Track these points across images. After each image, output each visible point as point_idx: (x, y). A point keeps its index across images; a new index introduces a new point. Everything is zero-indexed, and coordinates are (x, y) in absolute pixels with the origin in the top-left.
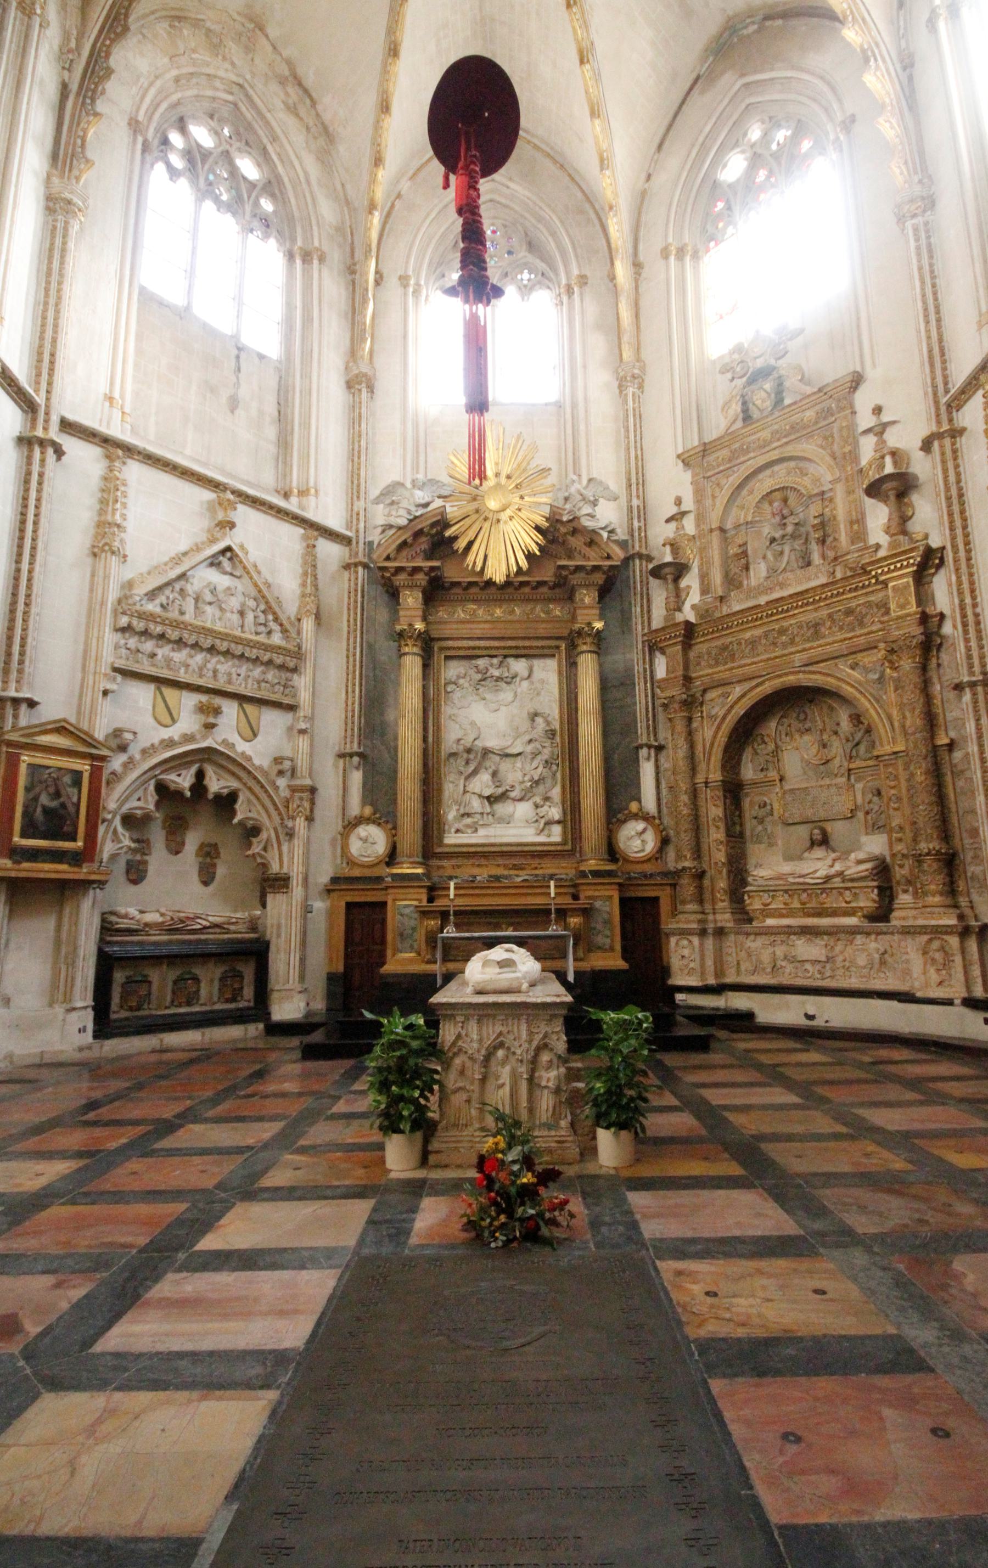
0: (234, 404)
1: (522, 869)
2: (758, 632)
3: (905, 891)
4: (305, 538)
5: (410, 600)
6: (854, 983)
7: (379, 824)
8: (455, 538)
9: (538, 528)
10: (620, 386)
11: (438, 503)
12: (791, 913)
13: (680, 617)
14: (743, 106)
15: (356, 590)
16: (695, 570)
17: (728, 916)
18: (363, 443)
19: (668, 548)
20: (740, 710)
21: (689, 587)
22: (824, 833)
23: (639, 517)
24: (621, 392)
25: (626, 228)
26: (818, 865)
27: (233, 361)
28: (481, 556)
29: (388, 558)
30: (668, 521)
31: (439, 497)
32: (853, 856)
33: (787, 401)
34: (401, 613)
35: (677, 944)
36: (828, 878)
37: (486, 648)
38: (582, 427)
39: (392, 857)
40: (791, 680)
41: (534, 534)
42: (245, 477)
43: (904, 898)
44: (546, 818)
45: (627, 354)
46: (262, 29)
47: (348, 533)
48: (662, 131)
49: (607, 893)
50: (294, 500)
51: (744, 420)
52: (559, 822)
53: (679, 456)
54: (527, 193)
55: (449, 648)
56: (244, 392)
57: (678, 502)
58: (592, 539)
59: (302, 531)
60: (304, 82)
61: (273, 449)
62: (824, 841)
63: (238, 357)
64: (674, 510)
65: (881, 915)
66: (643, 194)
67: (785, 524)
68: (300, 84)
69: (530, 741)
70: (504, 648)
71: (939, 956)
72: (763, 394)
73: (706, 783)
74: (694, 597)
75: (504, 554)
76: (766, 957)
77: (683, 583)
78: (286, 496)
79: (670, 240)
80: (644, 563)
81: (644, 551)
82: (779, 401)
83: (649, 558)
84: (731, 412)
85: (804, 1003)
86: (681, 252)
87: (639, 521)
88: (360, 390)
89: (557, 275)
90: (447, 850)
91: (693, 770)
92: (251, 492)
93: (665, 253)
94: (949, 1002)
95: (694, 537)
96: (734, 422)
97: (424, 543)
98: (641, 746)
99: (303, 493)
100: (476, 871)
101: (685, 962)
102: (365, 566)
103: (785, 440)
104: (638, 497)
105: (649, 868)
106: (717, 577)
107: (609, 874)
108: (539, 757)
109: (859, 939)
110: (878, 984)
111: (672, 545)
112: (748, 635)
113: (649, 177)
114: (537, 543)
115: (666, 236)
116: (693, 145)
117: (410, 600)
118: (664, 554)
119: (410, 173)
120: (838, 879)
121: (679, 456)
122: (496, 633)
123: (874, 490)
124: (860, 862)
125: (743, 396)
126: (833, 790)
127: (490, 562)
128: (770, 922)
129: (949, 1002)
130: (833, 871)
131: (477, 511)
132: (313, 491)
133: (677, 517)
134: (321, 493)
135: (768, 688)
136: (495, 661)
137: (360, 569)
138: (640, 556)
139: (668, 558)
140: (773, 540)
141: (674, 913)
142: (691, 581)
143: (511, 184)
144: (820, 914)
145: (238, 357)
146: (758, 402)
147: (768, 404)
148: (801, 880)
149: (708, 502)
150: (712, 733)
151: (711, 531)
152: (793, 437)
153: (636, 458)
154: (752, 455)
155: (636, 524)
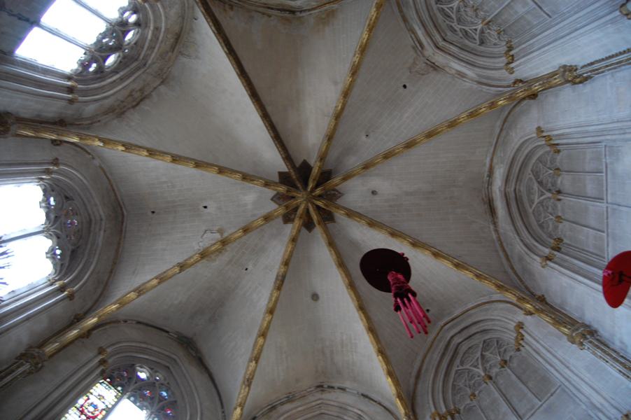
14: (168, 365)
46: (162, 83)
48: (145, 321)
54: (100, 244)
60: (142, 103)
63: (27, 20)
66: (117, 322)
68: (141, 100)
79: (109, 350)
93: (101, 351)
113: (126, 321)
115: (109, 347)
116: (145, 343)
119: (103, 166)
143: (102, 232)
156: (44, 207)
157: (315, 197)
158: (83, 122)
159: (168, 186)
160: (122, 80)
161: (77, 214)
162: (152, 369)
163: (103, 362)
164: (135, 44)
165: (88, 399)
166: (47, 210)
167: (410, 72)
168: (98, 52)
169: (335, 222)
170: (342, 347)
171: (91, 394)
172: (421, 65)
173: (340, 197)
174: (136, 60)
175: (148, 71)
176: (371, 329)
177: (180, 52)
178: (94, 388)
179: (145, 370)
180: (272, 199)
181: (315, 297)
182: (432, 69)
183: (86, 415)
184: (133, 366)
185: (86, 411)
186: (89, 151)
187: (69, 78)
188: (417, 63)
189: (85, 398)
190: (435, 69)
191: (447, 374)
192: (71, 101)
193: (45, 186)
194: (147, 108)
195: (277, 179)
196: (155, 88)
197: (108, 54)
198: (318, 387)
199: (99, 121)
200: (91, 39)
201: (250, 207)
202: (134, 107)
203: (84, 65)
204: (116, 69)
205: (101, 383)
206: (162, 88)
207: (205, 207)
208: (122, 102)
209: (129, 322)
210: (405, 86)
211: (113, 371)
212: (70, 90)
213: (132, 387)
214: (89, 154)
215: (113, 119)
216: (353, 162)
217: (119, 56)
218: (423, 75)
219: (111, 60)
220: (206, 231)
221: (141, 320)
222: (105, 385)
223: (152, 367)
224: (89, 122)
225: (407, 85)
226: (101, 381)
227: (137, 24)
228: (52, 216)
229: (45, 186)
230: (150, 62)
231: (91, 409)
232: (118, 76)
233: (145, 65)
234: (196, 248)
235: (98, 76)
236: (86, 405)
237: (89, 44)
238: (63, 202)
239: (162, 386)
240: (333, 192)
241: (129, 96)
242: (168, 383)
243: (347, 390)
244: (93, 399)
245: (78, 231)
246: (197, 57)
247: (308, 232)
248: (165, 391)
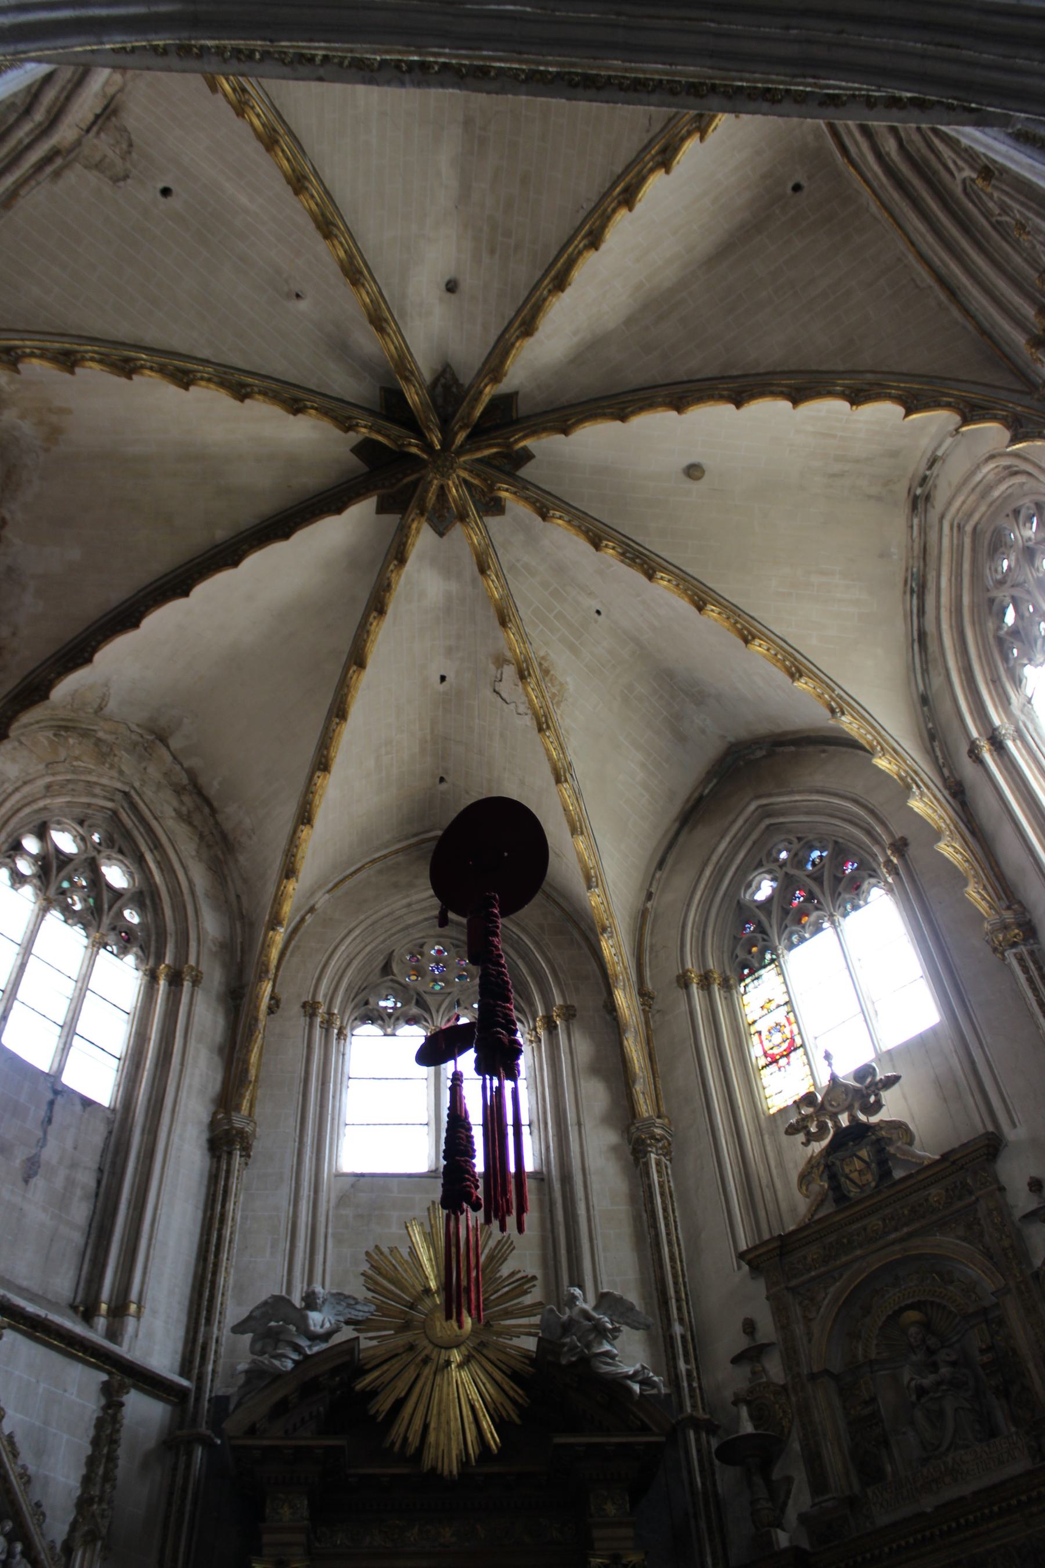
0: (31, 1169)
4: (107, 1389)
5: (286, 1512)
8: (372, 1394)
9: (515, 1376)
10: (635, 1152)
11: (347, 1333)
13: (783, 1539)
15: (184, 1490)
16: (796, 1446)
18: (227, 1233)
19: (744, 1412)
21: (789, 1480)
23: (686, 1355)
24: (637, 1160)
25: (627, 951)
27: (44, 1107)
28: (417, 1424)
29: (252, 1431)
31: (348, 1322)
34: (266, 1538)
38: (582, 1211)
41: (508, 1384)
42: (25, 1284)
45: (645, 1108)
47: (185, 1383)
50: (101, 1322)
51: (837, 1201)
53: (741, 1256)
56: (50, 1154)
57: (749, 1327)
59: (105, 1377)
61: (78, 1238)
63: (51, 1104)
64: (742, 1343)
66: (644, 913)
72: (858, 1164)
74: (800, 1500)
75: (455, 1425)
77: (776, 1475)
78: (88, 1315)
80: (704, 1435)
81: (701, 1414)
82: (885, 1174)
83: (711, 1428)
84: (815, 1187)
86: (706, 982)
87: (687, 1362)
88: (230, 1154)
89: (531, 1004)
92: (31, 1308)
95: (784, 1387)
96: (820, 1204)
99: (119, 1310)
102: (207, 1443)
103: (905, 1230)
104: (681, 1320)
106: (835, 1460)
111: (748, 1403)
113: (649, 896)
116: (705, 865)
117: (286, 1512)
118: (738, 1418)
121: (741, 1256)
125: (827, 1166)
127: (432, 1438)
131: (411, 1347)
132: (133, 1307)
133: (750, 1356)
134: (146, 1312)
137: (199, 1452)
138: (696, 1424)
139: (748, 1428)
140: (921, 1391)
142: (792, 1467)
145: (51, 1104)
146: (855, 1176)
149: (799, 1329)
151: (813, 1377)
152: (916, 1225)
153: (672, 1258)
154: (859, 1252)
155: (682, 1366)
156: (394, 1029)
157: (446, 443)
158: (239, 940)
159: (387, 753)
160: (156, 845)
161: (422, 946)
162: (760, 864)
163: (706, 982)
164: (81, 823)
165: (760, 1033)
166: (401, 1022)
167: (126, 177)
168: (99, 916)
169: (516, 393)
170: (834, 437)
171: (754, 1022)
172: (102, 145)
173: (453, 374)
174: (115, 813)
175: (137, 784)
176: (800, 389)
177: (96, 712)
178: (747, 1010)
179: (758, 879)
180: (441, 534)
181: (694, 471)
182: (113, 119)
183: (782, 1056)
184: (740, 906)
185: (776, 1051)
186: (298, 918)
187: (152, 977)
188: (98, 157)
189: (755, 1039)
190: (115, 112)
191: (965, 225)
192: (196, 982)
193: (356, 1019)
194: (216, 783)
195: (392, 520)
196: (175, 758)
197: (104, 888)
198: (914, 507)
199: (238, 897)
200: (76, 937)
201: (454, 587)
202: (214, 811)
203: (127, 940)
204: (136, 861)
205: (745, 992)
206: (176, 743)
207: (443, 678)
208: (201, 837)
209: (653, 890)
210: (166, 192)
211: (733, 956)
212: (175, 979)
213: (774, 933)
214: (302, 920)
215: (236, 861)
216: (366, 341)
217: (109, 858)
218: (131, 145)
219: (115, 876)
220: (495, 691)
221: (657, 858)
222: (751, 986)
223: (760, 860)
224: (238, 925)
225: (161, 185)
226: (742, 990)
227: (42, 833)
228: (415, 1010)
229: (356, 1019)
230: (119, 785)
231: (777, 1038)
232: (149, 858)
233: (126, 794)
234: (529, 723)
235: (148, 902)
236: (767, 1045)
237: (85, 942)
238: (392, 980)
239: (798, 860)
240: (439, 389)
241: (190, 823)
242: (799, 839)
243: (939, 453)
244: (763, 1026)
245: (456, 946)
246: (106, 685)
247: (533, 461)
248: (812, 852)
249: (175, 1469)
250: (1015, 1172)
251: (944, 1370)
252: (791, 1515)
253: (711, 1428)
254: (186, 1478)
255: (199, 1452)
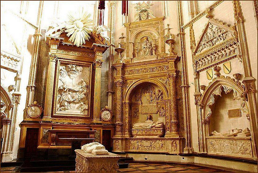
1: (77, 121)
2: (139, 68)
3: (168, 130)
6: (156, 151)
7: (39, 107)
9: (89, 34)
12: (143, 135)
17: (128, 135)
20: (134, 86)
22: (151, 116)
23: (113, 36)
26: (149, 124)
30: (120, 38)
32: (157, 122)
33: (149, 18)
35: (115, 142)
36: (152, 127)
37: (72, 62)
39: (42, 115)
40: (146, 80)
43: (168, 132)
44: (84, 108)
49: (100, 129)
52: (87, 110)
55: (62, 61)
57: (123, 34)
58: (103, 39)
62: (151, 118)
64: (121, 36)
65: (163, 135)
67: (147, 45)
69: (81, 88)
70: (77, 63)
71: (175, 145)
73: (125, 103)
74: (125, 58)
76: (136, 146)
85: (145, 156)
90: (56, 115)
91: (122, 99)
94: (176, 155)
97: (60, 33)
98: (109, 92)
100: (64, 121)
101: (117, 146)
105: (109, 123)
107: (101, 124)
108: (83, 93)
109: (158, 141)
110: (160, 151)
112: (137, 68)
114: (88, 38)
120: (154, 127)
122: (75, 59)
123: (167, 42)
124: (159, 124)
126: (153, 107)
128: (138, 137)
129: (176, 155)
130: (153, 125)
135: (141, 82)
136: (74, 66)
138: (112, 45)
141: (114, 134)
142: (125, 54)
144: (149, 135)
147: (145, 18)
148: (146, 127)
149: (130, 36)
150: (128, 90)
151: (130, 43)
249: (36, 39)
250: (166, 22)
251: (148, 46)
252: (123, 59)
253: (114, 46)
254: (38, 40)
255: (40, 37)
